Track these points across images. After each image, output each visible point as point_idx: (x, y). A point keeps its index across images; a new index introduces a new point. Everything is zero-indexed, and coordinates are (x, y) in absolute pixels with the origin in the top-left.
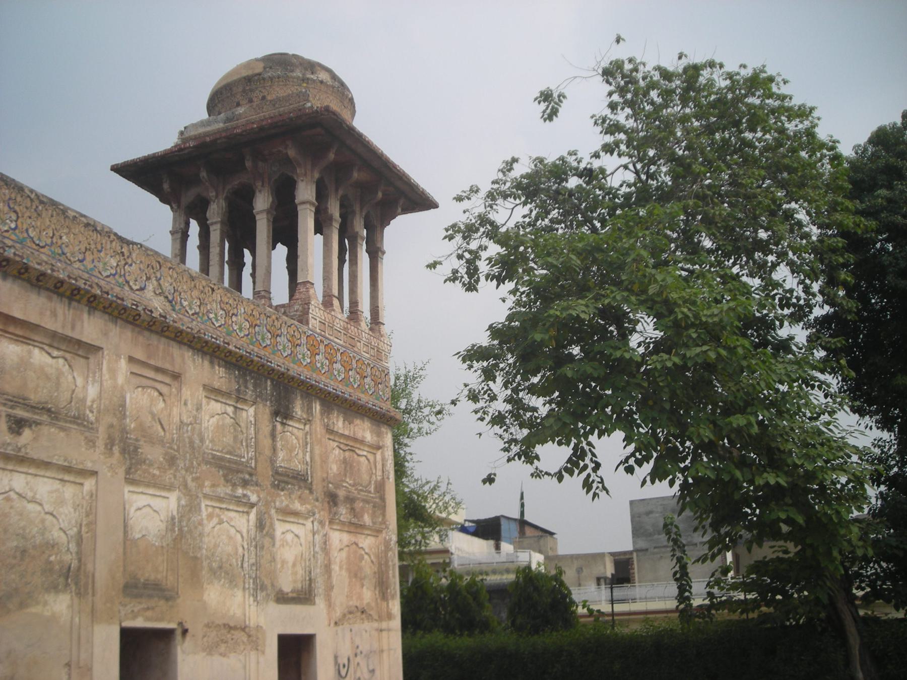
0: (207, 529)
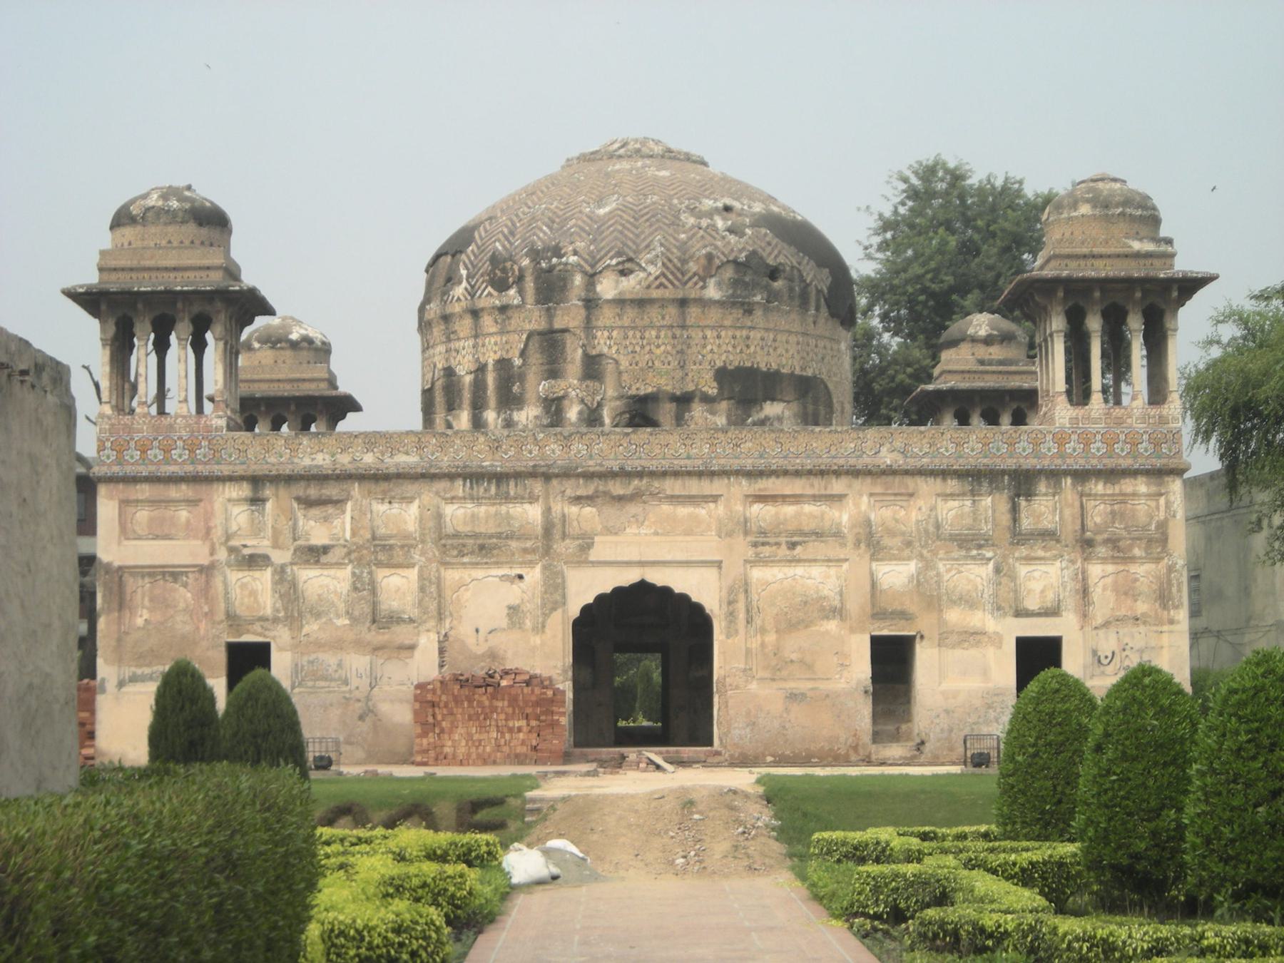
0: (946, 578)
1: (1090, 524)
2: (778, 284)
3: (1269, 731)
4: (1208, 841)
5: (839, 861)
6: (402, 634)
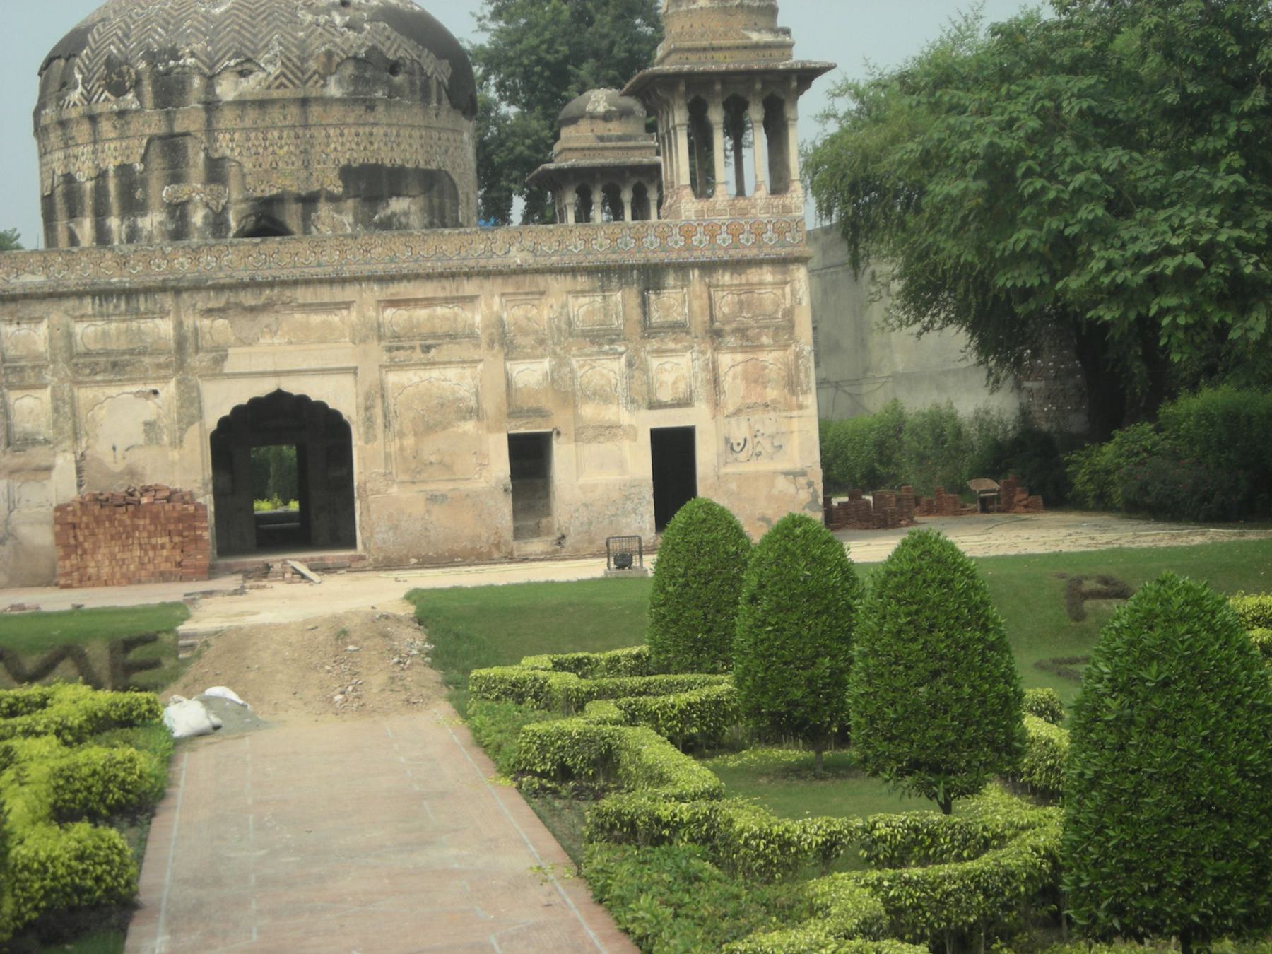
0: (580, 373)
1: (718, 314)
2: (399, 79)
3: (928, 613)
4: (872, 721)
5: (498, 698)
6: (38, 456)
